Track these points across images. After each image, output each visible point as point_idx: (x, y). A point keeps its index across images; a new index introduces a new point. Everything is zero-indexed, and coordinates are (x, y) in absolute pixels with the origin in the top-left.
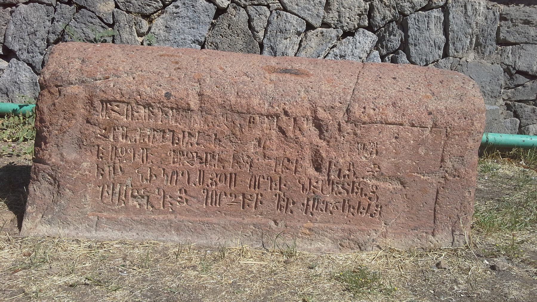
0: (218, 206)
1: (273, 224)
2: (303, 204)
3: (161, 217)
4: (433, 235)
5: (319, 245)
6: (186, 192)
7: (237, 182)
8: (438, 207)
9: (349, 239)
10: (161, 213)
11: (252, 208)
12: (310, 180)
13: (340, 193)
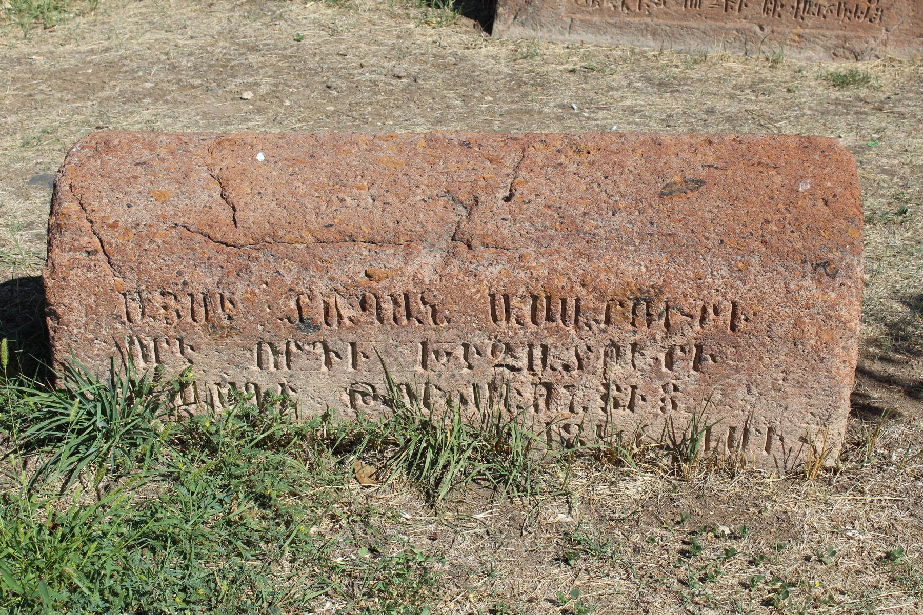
0: (698, 8)
1: (757, 29)
2: (793, 7)
3: (637, 20)
5: (810, 53)
9: (844, 48)
11: (735, 10)
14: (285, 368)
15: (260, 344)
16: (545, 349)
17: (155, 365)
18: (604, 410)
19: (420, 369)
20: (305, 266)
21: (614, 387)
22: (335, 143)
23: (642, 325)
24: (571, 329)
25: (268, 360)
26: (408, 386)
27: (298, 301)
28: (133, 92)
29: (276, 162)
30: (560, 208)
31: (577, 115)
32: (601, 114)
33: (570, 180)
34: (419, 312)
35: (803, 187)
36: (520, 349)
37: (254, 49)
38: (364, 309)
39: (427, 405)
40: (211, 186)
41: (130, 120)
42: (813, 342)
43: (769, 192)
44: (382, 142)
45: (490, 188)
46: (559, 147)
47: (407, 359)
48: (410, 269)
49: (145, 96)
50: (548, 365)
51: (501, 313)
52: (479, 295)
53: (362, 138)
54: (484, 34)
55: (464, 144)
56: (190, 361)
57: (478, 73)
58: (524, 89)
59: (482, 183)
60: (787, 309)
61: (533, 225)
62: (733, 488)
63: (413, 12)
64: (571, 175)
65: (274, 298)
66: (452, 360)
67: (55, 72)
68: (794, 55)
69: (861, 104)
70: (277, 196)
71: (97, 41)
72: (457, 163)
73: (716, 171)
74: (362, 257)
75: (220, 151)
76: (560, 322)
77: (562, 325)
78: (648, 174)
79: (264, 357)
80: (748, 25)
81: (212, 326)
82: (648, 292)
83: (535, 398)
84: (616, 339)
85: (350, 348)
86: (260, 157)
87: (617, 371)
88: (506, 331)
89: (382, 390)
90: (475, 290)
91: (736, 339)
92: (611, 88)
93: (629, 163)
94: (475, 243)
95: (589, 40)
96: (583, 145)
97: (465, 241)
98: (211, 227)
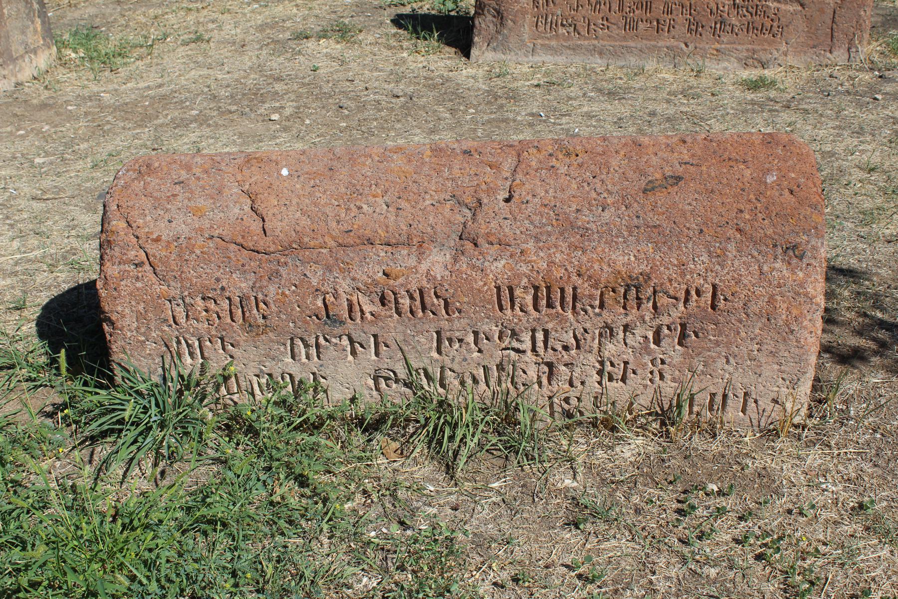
1: (683, 46)
2: (711, 27)
3: (586, 42)
4: (831, 52)
5: (726, 64)
6: (607, 20)
7: (652, 10)
8: (835, 26)
10: (588, 39)
12: (717, 4)
13: (745, 16)
14: (316, 358)
15: (292, 339)
16: (546, 333)
17: (201, 361)
18: (600, 383)
19: (435, 355)
20: (329, 269)
21: (608, 363)
22: (350, 156)
23: (632, 308)
24: (569, 314)
25: (300, 353)
26: (426, 371)
27: (324, 300)
28: (182, 119)
29: (299, 176)
30: (555, 206)
31: (545, 121)
32: (564, 120)
33: (562, 181)
34: (433, 305)
35: (770, 179)
36: (524, 334)
37: (279, 79)
38: (383, 304)
39: (443, 385)
40: (242, 200)
41: (179, 142)
42: (784, 317)
43: (740, 184)
44: (392, 154)
45: (491, 191)
46: (551, 151)
47: (424, 347)
48: (423, 267)
49: (191, 122)
50: (549, 346)
51: (506, 303)
52: (486, 288)
53: (375, 150)
54: (463, 59)
55: (465, 152)
56: (232, 357)
57: (461, 91)
58: (500, 101)
59: (484, 187)
60: (761, 289)
61: (532, 223)
62: (715, 447)
63: (405, 44)
64: (563, 176)
65: (303, 298)
66: (464, 346)
67: (119, 106)
68: (713, 66)
69: (772, 103)
70: (302, 207)
71: (153, 79)
72: (461, 169)
73: (692, 167)
74: (380, 258)
75: (249, 168)
76: (559, 308)
77: (561, 311)
78: (632, 173)
79: (296, 350)
80: (676, 43)
81: (249, 325)
82: (637, 278)
83: (538, 375)
84: (609, 321)
85: (372, 339)
86: (285, 172)
87: (611, 349)
88: (511, 318)
89: (402, 374)
90: (482, 283)
91: (716, 317)
92: (570, 98)
93: (614, 163)
94: (480, 241)
95: (548, 60)
96: (571, 149)
97: (471, 240)
98: (243, 237)
